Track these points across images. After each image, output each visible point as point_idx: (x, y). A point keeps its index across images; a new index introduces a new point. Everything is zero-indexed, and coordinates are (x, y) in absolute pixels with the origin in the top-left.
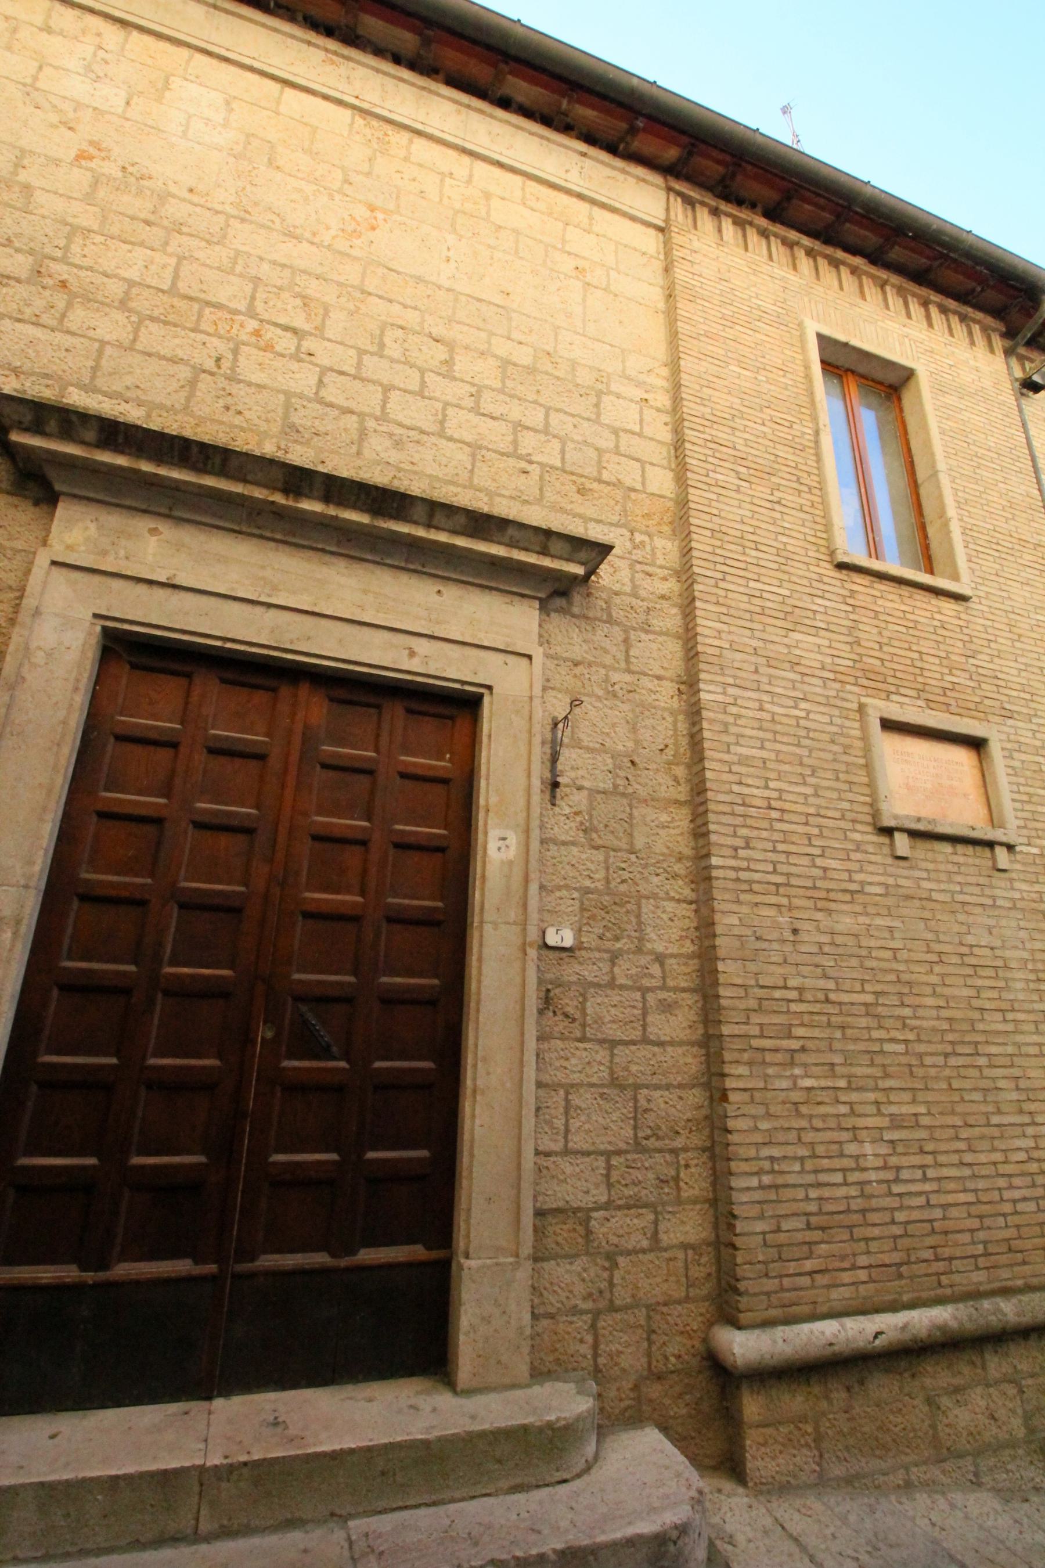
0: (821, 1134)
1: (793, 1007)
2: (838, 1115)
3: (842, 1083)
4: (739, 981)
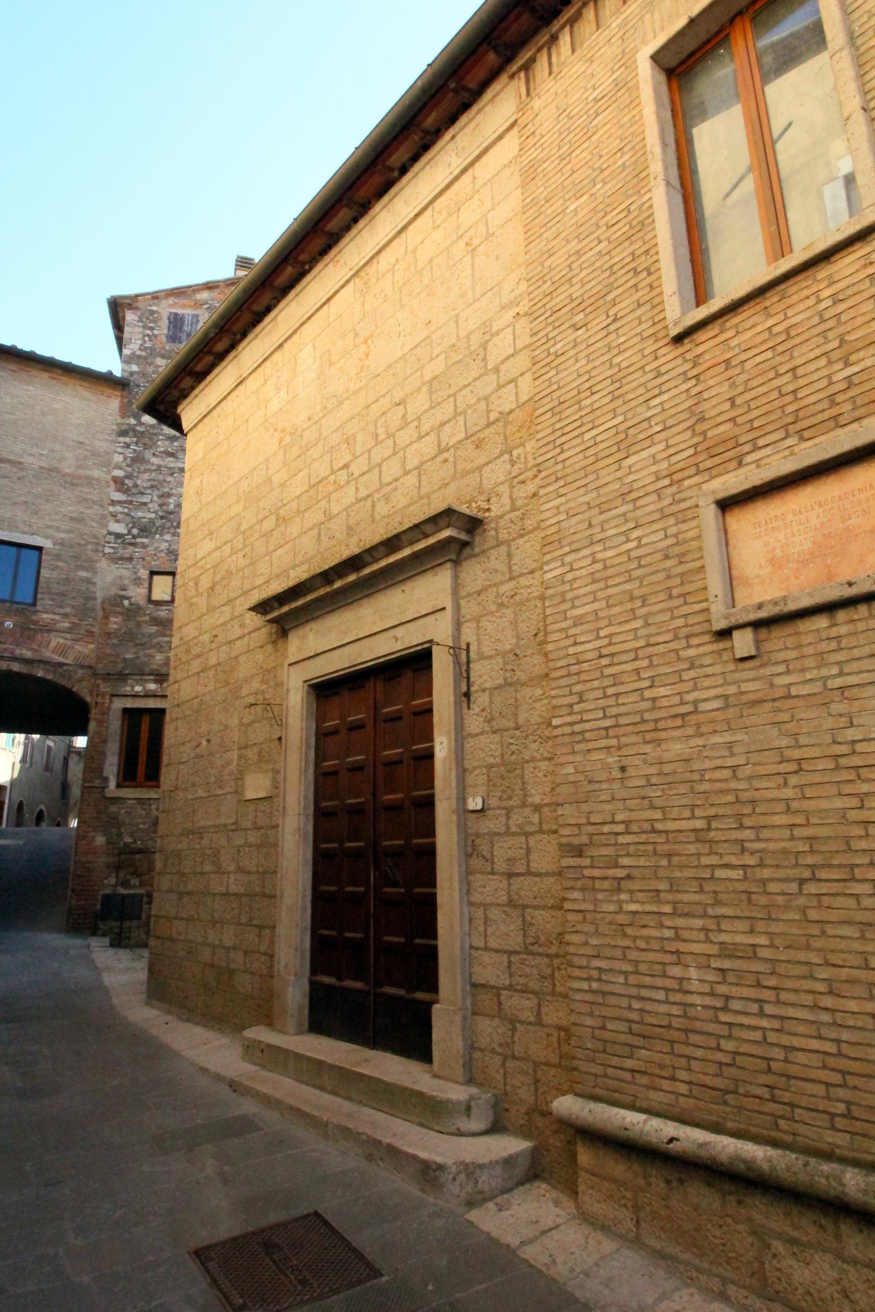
0: (644, 954)
1: (621, 839)
2: (663, 939)
3: (668, 909)
4: (573, 822)
